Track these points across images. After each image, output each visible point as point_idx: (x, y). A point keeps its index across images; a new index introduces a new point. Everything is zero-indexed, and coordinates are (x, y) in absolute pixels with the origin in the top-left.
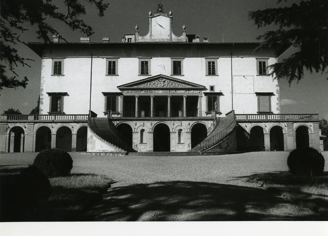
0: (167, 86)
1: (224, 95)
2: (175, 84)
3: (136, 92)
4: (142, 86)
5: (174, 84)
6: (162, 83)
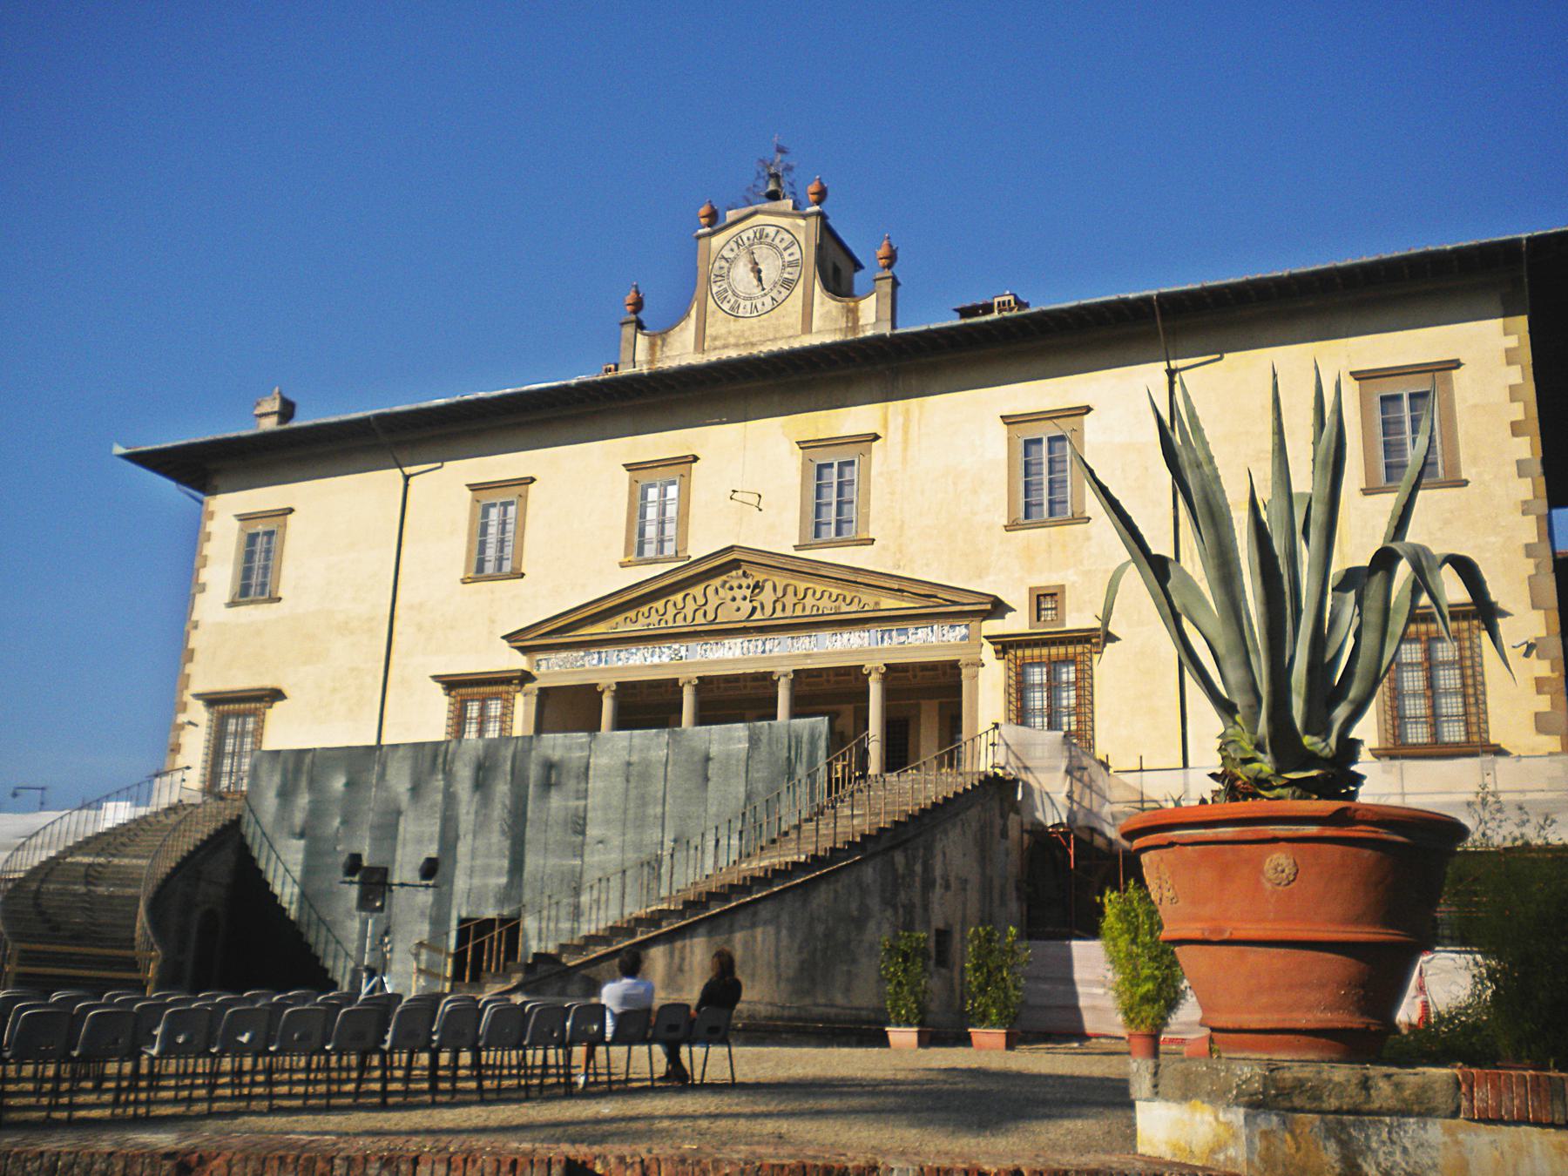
0: (774, 612)
1: (1118, 639)
2: (818, 595)
3: (600, 660)
4: (620, 625)
5: (809, 601)
6: (745, 598)
